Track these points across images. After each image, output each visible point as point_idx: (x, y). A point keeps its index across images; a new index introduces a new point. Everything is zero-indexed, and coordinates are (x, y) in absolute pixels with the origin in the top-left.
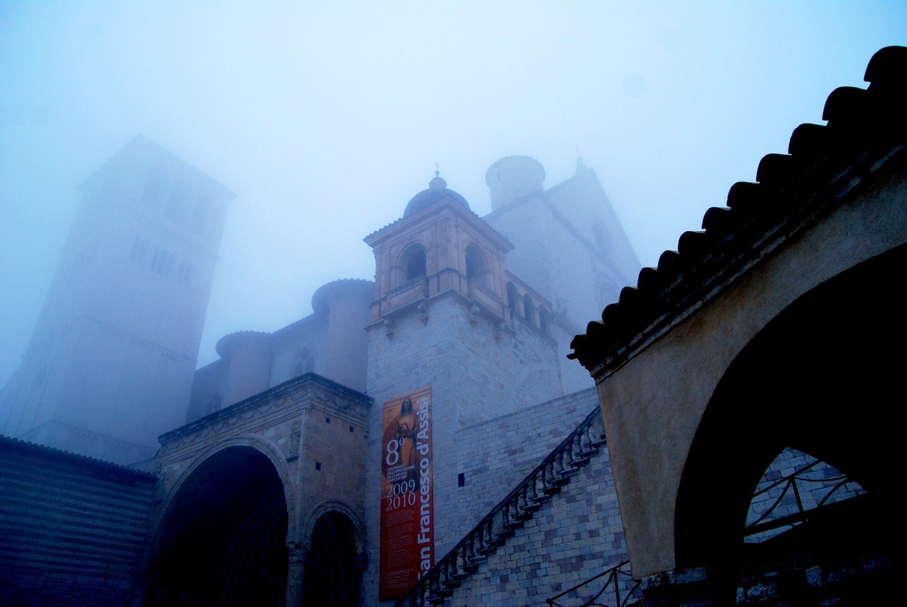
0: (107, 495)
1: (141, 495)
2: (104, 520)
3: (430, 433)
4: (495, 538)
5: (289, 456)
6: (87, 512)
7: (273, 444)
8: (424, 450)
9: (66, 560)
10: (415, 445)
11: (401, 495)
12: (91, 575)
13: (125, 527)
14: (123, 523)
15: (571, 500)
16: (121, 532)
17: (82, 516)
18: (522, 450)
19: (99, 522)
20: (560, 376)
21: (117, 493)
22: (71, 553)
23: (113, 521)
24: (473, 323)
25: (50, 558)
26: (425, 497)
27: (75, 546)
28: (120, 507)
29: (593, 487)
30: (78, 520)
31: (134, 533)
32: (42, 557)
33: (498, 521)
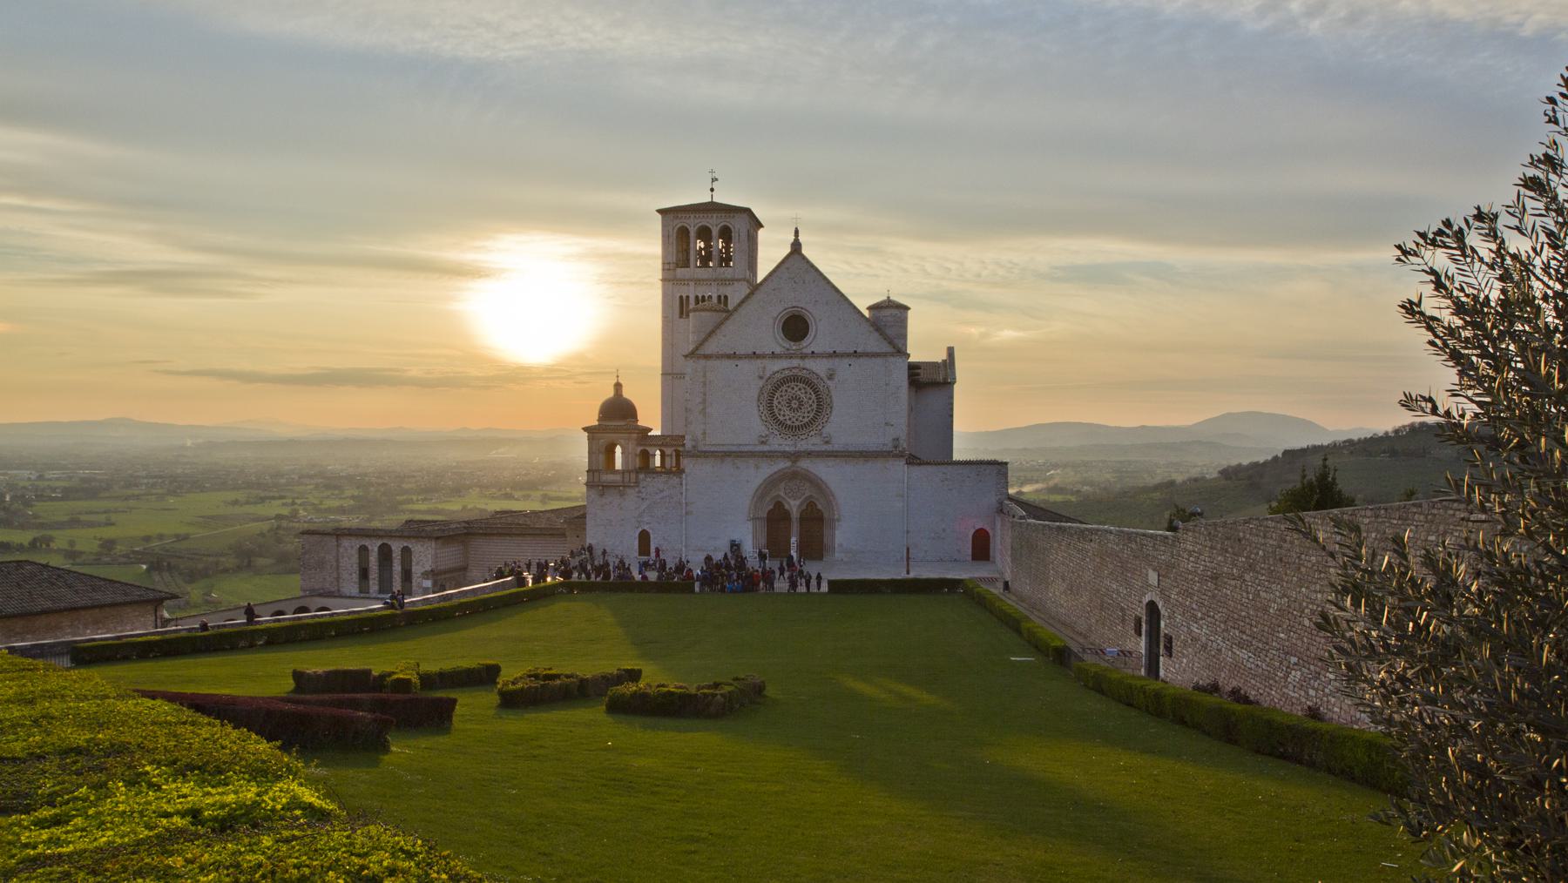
20: (682, 493)
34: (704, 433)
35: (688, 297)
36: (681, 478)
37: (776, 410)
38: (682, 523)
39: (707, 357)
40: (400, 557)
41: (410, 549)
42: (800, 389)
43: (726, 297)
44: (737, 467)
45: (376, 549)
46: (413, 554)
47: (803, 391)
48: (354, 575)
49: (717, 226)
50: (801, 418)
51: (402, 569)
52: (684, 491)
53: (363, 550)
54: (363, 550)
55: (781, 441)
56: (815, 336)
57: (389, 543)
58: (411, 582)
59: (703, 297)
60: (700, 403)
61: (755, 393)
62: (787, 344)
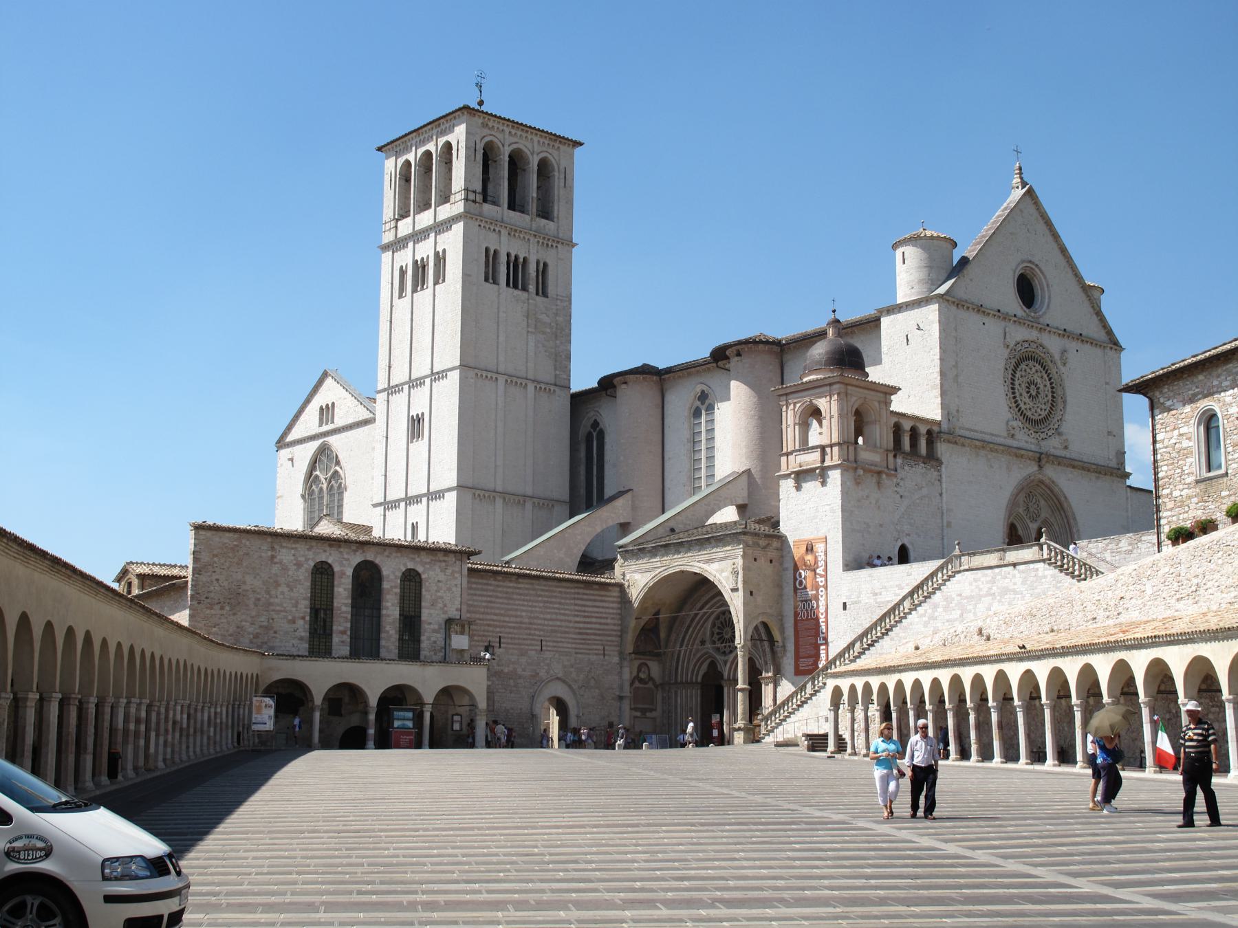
0: (595, 601)
1: (614, 597)
2: (596, 617)
3: (826, 570)
4: (856, 654)
5: (731, 587)
6: (586, 614)
7: (718, 575)
8: (822, 582)
9: (581, 646)
10: (816, 578)
11: (807, 610)
12: (596, 654)
13: (609, 621)
14: (607, 618)
15: (892, 639)
16: (607, 624)
17: (585, 617)
18: (881, 594)
19: (594, 620)
20: (941, 495)
21: (600, 598)
22: (583, 641)
23: (601, 618)
24: (858, 484)
25: (574, 646)
26: (822, 614)
27: (585, 637)
28: (603, 607)
29: (902, 635)
30: (582, 619)
31: (614, 625)
32: (569, 645)
33: (858, 645)
34: (958, 411)
35: (496, 252)
36: (939, 471)
37: (1017, 394)
38: (943, 539)
39: (960, 304)
40: (398, 590)
41: (419, 574)
42: (1037, 372)
43: (545, 265)
44: (992, 467)
45: (349, 572)
46: (425, 585)
47: (1039, 374)
48: (301, 622)
49: (538, 154)
50: (1039, 410)
51: (400, 615)
52: (944, 491)
53: (323, 573)
54: (323, 573)
55: (1026, 438)
56: (1048, 306)
57: (377, 561)
58: (419, 641)
59: (516, 257)
60: (954, 366)
61: (1001, 366)
62: (1027, 311)
